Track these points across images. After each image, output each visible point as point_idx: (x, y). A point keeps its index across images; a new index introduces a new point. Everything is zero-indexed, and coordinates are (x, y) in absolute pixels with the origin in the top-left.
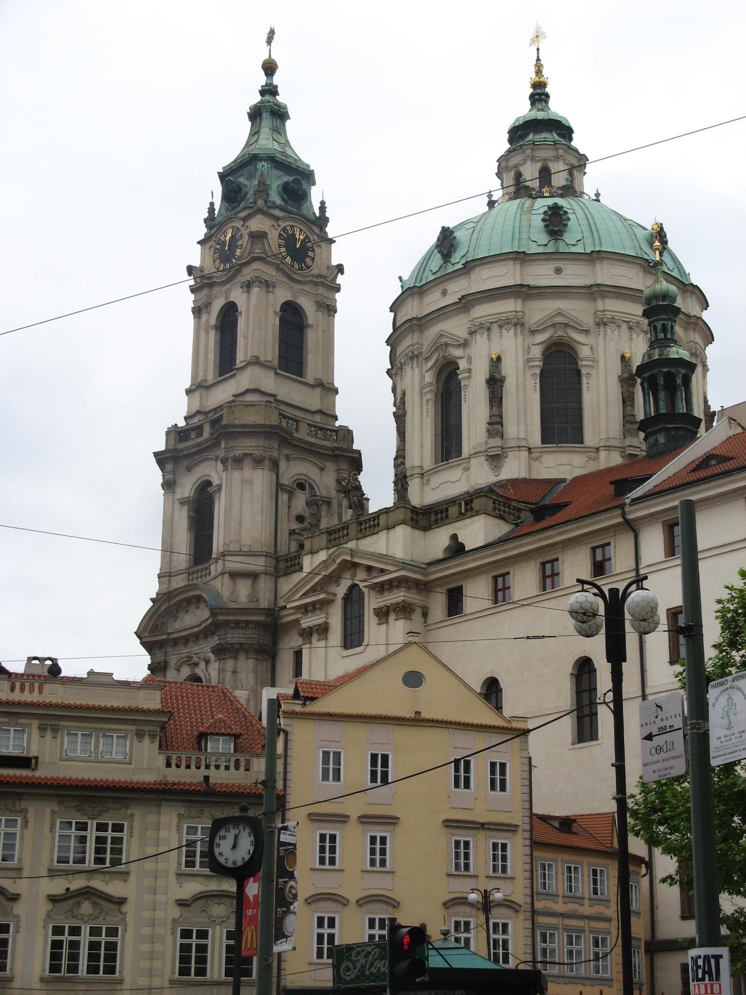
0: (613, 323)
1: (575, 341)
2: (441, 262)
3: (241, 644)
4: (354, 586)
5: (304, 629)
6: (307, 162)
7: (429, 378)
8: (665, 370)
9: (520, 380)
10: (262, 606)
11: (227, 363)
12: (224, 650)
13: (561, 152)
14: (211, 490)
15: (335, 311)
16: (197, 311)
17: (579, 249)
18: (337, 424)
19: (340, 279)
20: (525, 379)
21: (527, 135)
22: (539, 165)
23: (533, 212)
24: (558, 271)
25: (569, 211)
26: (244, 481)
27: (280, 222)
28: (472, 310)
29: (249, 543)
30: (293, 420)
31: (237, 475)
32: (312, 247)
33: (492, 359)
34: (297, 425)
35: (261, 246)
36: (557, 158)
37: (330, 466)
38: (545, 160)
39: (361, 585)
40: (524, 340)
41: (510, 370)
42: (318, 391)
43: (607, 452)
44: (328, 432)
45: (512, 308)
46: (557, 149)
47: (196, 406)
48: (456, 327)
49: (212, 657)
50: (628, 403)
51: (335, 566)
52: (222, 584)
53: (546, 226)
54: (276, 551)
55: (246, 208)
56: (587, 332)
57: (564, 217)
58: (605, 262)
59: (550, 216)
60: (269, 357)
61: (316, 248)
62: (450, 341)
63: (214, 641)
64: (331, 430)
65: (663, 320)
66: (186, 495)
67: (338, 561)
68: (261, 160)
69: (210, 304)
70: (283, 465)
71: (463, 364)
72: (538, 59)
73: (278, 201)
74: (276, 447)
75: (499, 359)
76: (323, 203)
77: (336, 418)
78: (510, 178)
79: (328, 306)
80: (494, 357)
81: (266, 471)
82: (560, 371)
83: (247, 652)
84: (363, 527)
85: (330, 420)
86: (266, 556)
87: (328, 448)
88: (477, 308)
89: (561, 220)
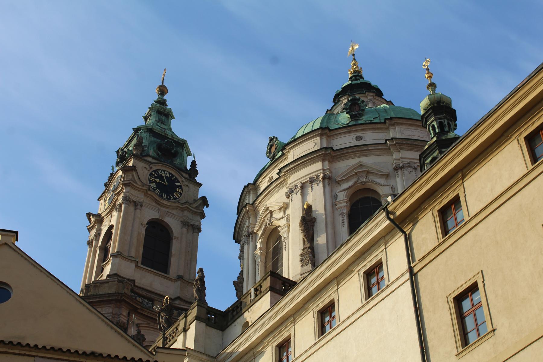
0: (409, 166)
6: (182, 138)
9: (329, 219)
15: (200, 230)
20: (334, 218)
24: (359, 138)
27: (151, 165)
40: (332, 191)
56: (387, 176)
57: (362, 105)
58: (398, 128)
60: (133, 254)
61: (184, 188)
65: (440, 119)
72: (354, 59)
73: (152, 152)
74: (125, 313)
89: (360, 107)
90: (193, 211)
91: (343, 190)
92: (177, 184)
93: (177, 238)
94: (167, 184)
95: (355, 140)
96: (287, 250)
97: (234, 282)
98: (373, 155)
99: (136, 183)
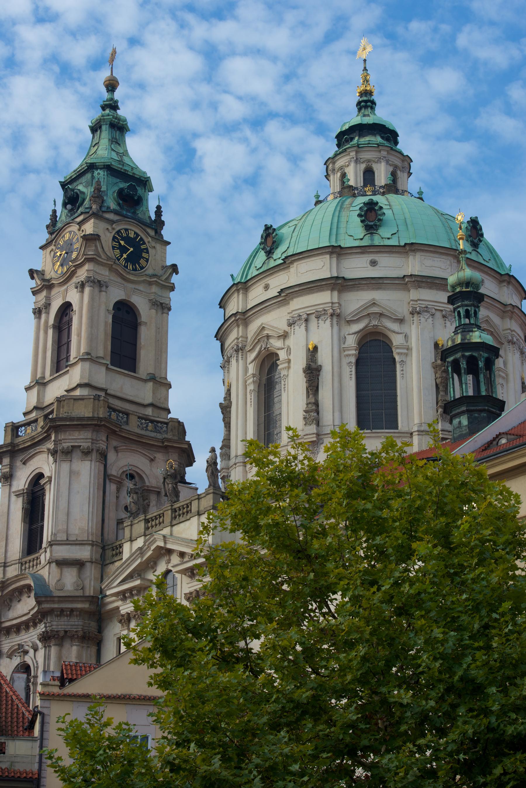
0: (426, 311)
1: (389, 330)
2: (265, 258)
3: (66, 632)
4: (168, 572)
5: (123, 616)
6: (144, 170)
7: (252, 369)
8: (467, 354)
10: (87, 594)
11: (60, 362)
12: (49, 638)
13: (384, 153)
14: (42, 482)
15: (169, 309)
16: (38, 312)
17: (393, 242)
18: (170, 416)
19: (175, 279)
20: (340, 367)
21: (352, 139)
22: (363, 166)
23: (351, 209)
24: (374, 263)
25: (384, 207)
26: (71, 473)
27: (114, 226)
28: (291, 302)
29: (77, 532)
30: (123, 413)
31: (65, 467)
32: (147, 249)
33: (309, 349)
34: (127, 418)
35: (94, 248)
36: (378, 161)
37: (160, 456)
38: (369, 161)
39: (174, 570)
40: (340, 330)
41: (325, 359)
42: (150, 384)
43: (420, 437)
44: (159, 425)
45: (328, 300)
46: (380, 151)
47: (34, 402)
48: (275, 319)
49: (40, 645)
50: (441, 388)
51: (150, 552)
52: (49, 573)
53: (362, 221)
54: (102, 540)
55: (82, 213)
56: (401, 321)
57: (379, 212)
59: (367, 211)
60: (101, 354)
61: (150, 250)
62: (270, 333)
63: (41, 628)
64: (161, 423)
66: (21, 487)
67: (153, 548)
68: (97, 169)
69: (50, 304)
70: (111, 456)
71: (282, 355)
72: (365, 69)
75: (316, 348)
76: (159, 208)
77: (169, 412)
78: (336, 178)
79: (161, 304)
80: (311, 347)
81: (93, 463)
82: (375, 360)
83: (72, 638)
84: (177, 514)
85: (163, 413)
86: (92, 545)
87: (157, 440)
88: (295, 300)
89: (377, 215)
90: (162, 284)
91: (353, 334)
92: (143, 247)
93: (146, 323)
94: (132, 249)
95: (369, 266)
96: (286, 391)
97: (221, 404)
98: (388, 289)
99: (100, 257)
